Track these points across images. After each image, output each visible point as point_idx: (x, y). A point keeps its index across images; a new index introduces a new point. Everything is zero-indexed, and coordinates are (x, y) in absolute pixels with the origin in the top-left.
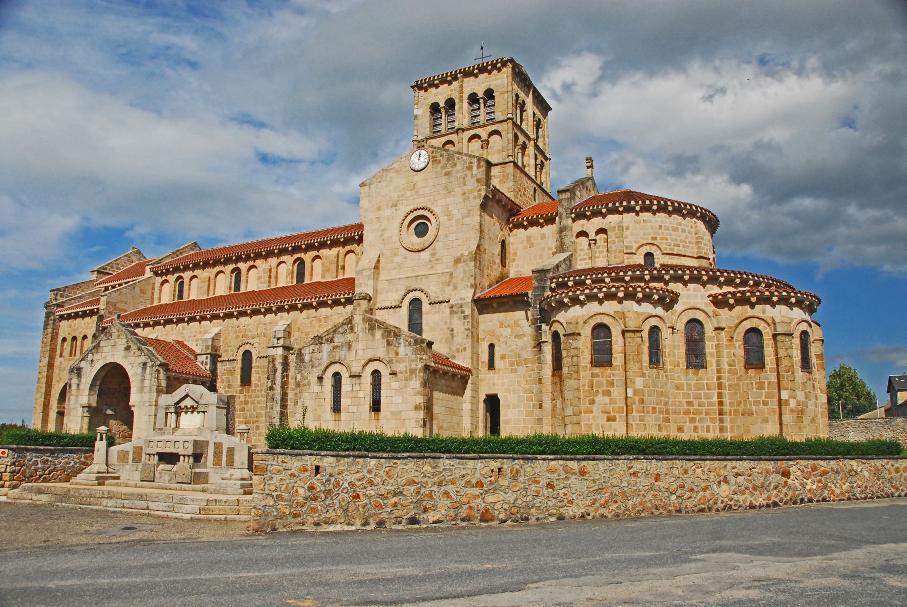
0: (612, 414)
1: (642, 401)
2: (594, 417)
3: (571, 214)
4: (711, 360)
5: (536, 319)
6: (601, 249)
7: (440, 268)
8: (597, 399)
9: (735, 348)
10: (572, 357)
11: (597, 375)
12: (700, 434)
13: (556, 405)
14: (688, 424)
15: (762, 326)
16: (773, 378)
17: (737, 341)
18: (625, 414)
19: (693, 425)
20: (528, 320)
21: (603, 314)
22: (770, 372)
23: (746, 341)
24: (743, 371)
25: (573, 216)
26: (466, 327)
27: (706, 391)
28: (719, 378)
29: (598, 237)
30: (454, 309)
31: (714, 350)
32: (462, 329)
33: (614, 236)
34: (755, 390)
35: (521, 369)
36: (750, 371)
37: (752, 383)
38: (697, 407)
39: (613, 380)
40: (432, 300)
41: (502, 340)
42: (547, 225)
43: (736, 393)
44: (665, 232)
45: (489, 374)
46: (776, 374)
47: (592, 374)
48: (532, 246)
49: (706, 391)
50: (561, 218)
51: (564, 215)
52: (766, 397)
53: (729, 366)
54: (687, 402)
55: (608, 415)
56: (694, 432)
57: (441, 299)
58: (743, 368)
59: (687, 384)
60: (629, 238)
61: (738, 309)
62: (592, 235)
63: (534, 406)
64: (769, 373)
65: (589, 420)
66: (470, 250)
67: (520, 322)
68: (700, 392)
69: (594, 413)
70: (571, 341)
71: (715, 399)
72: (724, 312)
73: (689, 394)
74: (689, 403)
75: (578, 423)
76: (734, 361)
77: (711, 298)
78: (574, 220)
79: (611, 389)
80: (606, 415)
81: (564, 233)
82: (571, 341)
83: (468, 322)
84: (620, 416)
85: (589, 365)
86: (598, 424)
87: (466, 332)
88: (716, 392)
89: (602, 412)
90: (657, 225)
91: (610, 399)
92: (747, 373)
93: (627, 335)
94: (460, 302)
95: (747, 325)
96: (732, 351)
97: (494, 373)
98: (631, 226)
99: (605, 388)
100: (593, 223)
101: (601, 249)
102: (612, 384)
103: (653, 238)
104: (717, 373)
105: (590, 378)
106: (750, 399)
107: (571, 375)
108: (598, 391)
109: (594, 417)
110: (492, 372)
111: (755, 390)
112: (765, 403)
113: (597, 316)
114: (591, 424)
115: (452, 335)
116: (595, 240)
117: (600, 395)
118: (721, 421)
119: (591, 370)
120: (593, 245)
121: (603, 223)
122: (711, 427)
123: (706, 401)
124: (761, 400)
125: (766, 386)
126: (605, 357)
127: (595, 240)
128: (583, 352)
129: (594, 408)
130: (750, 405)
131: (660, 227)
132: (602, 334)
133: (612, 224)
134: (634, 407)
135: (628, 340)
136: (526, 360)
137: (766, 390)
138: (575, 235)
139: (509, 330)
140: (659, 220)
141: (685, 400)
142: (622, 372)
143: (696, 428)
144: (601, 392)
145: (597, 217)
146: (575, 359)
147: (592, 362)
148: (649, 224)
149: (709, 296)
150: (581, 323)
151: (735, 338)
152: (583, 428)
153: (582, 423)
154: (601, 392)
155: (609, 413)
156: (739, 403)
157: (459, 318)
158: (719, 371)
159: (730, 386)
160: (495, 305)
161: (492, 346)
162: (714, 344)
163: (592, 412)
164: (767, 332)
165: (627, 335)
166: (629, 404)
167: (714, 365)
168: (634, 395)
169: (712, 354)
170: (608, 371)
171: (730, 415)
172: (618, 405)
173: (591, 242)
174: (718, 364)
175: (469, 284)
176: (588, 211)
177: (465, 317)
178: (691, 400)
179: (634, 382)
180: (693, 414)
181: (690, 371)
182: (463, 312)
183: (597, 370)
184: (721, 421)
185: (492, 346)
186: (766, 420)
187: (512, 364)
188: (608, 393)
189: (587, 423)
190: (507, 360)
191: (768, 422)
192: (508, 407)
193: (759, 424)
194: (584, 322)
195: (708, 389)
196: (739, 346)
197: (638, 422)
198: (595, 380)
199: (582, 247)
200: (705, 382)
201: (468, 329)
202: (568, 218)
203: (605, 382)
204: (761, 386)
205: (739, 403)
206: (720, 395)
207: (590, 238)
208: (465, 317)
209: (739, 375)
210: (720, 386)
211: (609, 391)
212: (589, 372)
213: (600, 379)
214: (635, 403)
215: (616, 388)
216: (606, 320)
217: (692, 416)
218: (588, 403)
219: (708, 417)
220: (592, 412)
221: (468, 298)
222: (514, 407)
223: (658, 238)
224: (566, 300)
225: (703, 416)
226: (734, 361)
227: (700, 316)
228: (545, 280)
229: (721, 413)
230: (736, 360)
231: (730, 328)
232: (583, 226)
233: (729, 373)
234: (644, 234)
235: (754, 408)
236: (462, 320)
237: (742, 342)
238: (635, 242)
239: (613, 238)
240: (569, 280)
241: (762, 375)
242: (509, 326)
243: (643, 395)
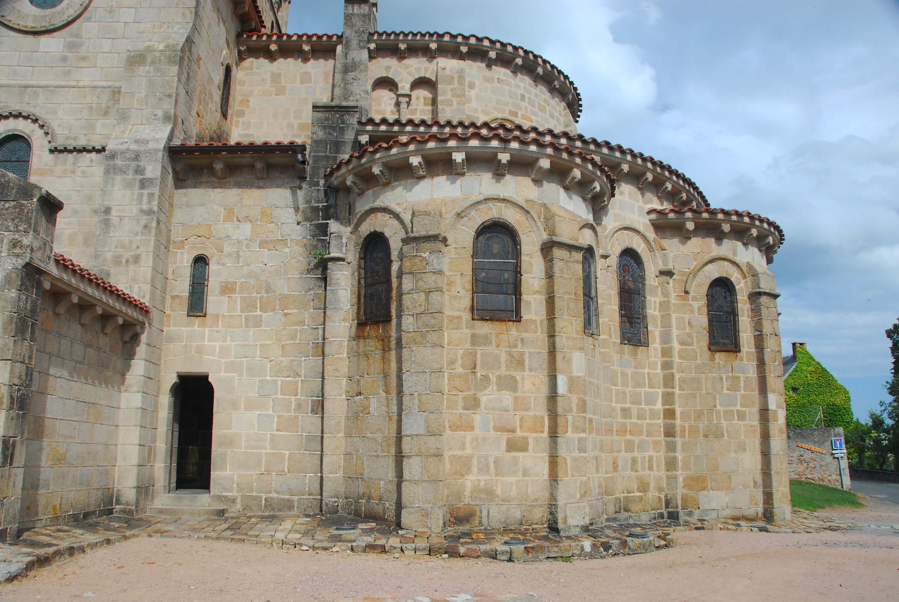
0: (519, 433)
1: (583, 406)
2: (475, 439)
3: (369, 41)
4: (655, 330)
5: (316, 209)
7: (86, 77)
8: (484, 399)
9: (692, 311)
10: (428, 292)
11: (486, 340)
12: (641, 473)
13: (366, 410)
14: (623, 453)
15: (735, 276)
16: (751, 371)
17: (695, 299)
18: (546, 434)
19: (629, 455)
20: (297, 209)
21: (504, 200)
22: (748, 360)
23: (711, 297)
24: (707, 354)
25: (372, 46)
26: (145, 207)
27: (647, 389)
28: (667, 366)
29: (414, 94)
30: (119, 162)
31: (657, 313)
32: (135, 210)
33: (450, 93)
34: (725, 391)
35: (272, 320)
36: (717, 355)
37: (721, 379)
38: (636, 421)
39: (522, 354)
40: (60, 143)
41: (227, 249)
42: (316, 58)
43: (694, 396)
44: (530, 108)
45: (189, 325)
46: (755, 363)
47: (473, 336)
48: (280, 92)
49: (647, 389)
50: (347, 47)
51: (354, 43)
52: (742, 405)
53: (681, 344)
54: (623, 410)
55: (511, 435)
56: (632, 470)
57: (82, 142)
58: (706, 349)
59: (622, 373)
60: (474, 104)
61: (696, 243)
62: (404, 87)
63: (299, 406)
64: (745, 361)
65: (463, 447)
66: (171, 42)
67: (277, 212)
68: (639, 389)
69: (477, 432)
70: (426, 255)
71: (659, 406)
72: (672, 245)
73: (624, 393)
74: (626, 412)
75: (438, 455)
76: (689, 336)
77: (653, 216)
78: (371, 58)
79: (518, 376)
80: (505, 436)
81: (351, 75)
82: (426, 255)
83: (151, 195)
84: (537, 440)
85: (467, 316)
86: (486, 458)
87: (144, 220)
88: (660, 391)
89: (496, 429)
90: (519, 92)
91: (516, 399)
92: (713, 359)
93: (557, 253)
94: (134, 147)
95: (714, 272)
96: (687, 317)
97: (202, 325)
98: (477, 83)
99: (503, 371)
100: (407, 67)
102: (520, 363)
103: (511, 113)
104: (663, 355)
105: (468, 346)
106: (718, 407)
107: (423, 335)
108: (486, 378)
109: (475, 439)
110: (197, 321)
111: (725, 391)
112: (741, 416)
113: (491, 204)
114: (470, 458)
115: (107, 223)
116: (409, 96)
117: (493, 387)
118: (671, 447)
119: (473, 327)
120: (404, 106)
121: (426, 69)
122: (655, 459)
123: (647, 408)
124: (735, 409)
125: (742, 384)
126: (501, 300)
128: (450, 284)
129: (477, 419)
130: (718, 418)
131: (523, 97)
132: (496, 248)
133: (448, 72)
134: (570, 418)
135: (558, 265)
136: (283, 297)
137: (743, 392)
138: (370, 82)
139: (246, 229)
140: (522, 85)
141: (619, 406)
142: (541, 335)
143: (634, 461)
144: (493, 379)
145: (416, 56)
146: (435, 296)
147: (472, 309)
148: (507, 88)
149: (649, 212)
150: (449, 216)
151: (692, 294)
152: (448, 465)
153: (447, 454)
154: (493, 379)
155: (513, 431)
156: (699, 415)
157: (129, 185)
158: (666, 352)
159: (683, 381)
160: (218, 166)
161: (201, 261)
162: (658, 300)
163: (472, 428)
164: (742, 288)
165: (557, 253)
166: (560, 411)
167: (658, 340)
168: (570, 391)
169: (655, 318)
170: (512, 331)
171: (683, 436)
172: (531, 413)
173: (402, 99)
174: (666, 338)
175: (160, 113)
176: (403, 42)
177: (143, 184)
178: (628, 405)
179: (569, 362)
180: (631, 434)
181: (627, 348)
182: (139, 171)
183: (485, 328)
184: (671, 447)
185: (201, 261)
186: (742, 448)
187: (249, 306)
188: (510, 384)
189: (458, 453)
190: (237, 296)
191: (745, 450)
192: (235, 406)
193: (733, 455)
194: (459, 216)
195: (650, 387)
196: (699, 309)
197: (576, 453)
198: (480, 350)
200: (647, 370)
201: (150, 212)
202: (362, 48)
203: (504, 357)
204: (734, 387)
205: (699, 415)
206: (668, 398)
207: (400, 92)
208: (143, 184)
209: (698, 362)
210: (668, 381)
211: (513, 378)
212: (466, 332)
213: (492, 349)
214: (570, 411)
215: (527, 373)
216: (511, 216)
217: (629, 437)
218: (461, 404)
219: (650, 439)
220: (472, 428)
221: (157, 140)
222: (249, 408)
223: (519, 115)
224: (415, 161)
225: (644, 437)
226: (689, 336)
227: (639, 246)
228: (342, 130)
229: (669, 432)
230: (695, 335)
231: (682, 273)
232: (388, 68)
233: (681, 357)
234: (498, 103)
235: (724, 424)
236: (136, 191)
237: (703, 302)
238: (483, 111)
239: (449, 96)
240: (402, 133)
241: (736, 363)
242: (247, 218)
243: (585, 393)
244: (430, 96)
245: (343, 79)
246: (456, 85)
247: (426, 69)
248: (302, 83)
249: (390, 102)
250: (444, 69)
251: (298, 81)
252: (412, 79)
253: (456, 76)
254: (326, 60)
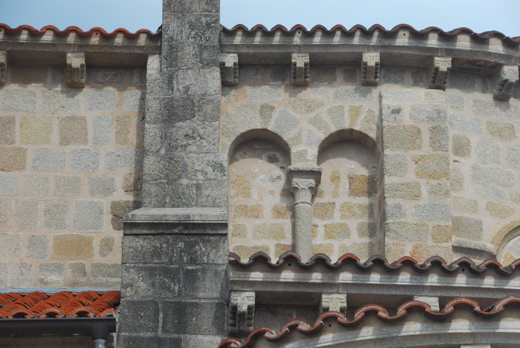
3: (222, 48)
6: (337, 218)
42: (100, 85)
81: (185, 126)
98: (474, 140)
101: (337, 218)
116: (316, 175)
120: (303, 197)
121: (355, 111)
127: (316, 175)
133: (406, 119)
138: (228, 142)
176: (300, 48)
199: (254, 200)
202: (207, 64)
207: (296, 165)
239: (410, 176)
244: (363, 172)
245: (165, 137)
246: (426, 149)
247: (355, 111)
248: (65, 141)
249: (270, 186)
250: (397, 111)
251: (55, 137)
252: (322, 136)
253: (425, 128)
254: (122, 87)
